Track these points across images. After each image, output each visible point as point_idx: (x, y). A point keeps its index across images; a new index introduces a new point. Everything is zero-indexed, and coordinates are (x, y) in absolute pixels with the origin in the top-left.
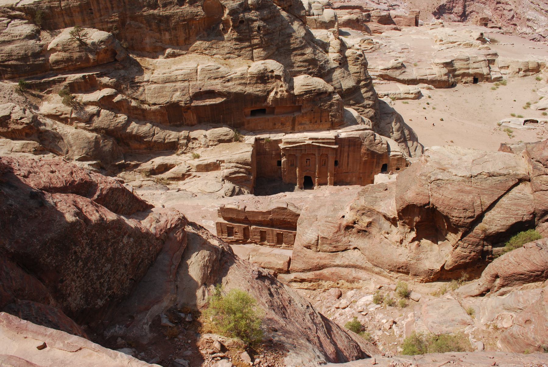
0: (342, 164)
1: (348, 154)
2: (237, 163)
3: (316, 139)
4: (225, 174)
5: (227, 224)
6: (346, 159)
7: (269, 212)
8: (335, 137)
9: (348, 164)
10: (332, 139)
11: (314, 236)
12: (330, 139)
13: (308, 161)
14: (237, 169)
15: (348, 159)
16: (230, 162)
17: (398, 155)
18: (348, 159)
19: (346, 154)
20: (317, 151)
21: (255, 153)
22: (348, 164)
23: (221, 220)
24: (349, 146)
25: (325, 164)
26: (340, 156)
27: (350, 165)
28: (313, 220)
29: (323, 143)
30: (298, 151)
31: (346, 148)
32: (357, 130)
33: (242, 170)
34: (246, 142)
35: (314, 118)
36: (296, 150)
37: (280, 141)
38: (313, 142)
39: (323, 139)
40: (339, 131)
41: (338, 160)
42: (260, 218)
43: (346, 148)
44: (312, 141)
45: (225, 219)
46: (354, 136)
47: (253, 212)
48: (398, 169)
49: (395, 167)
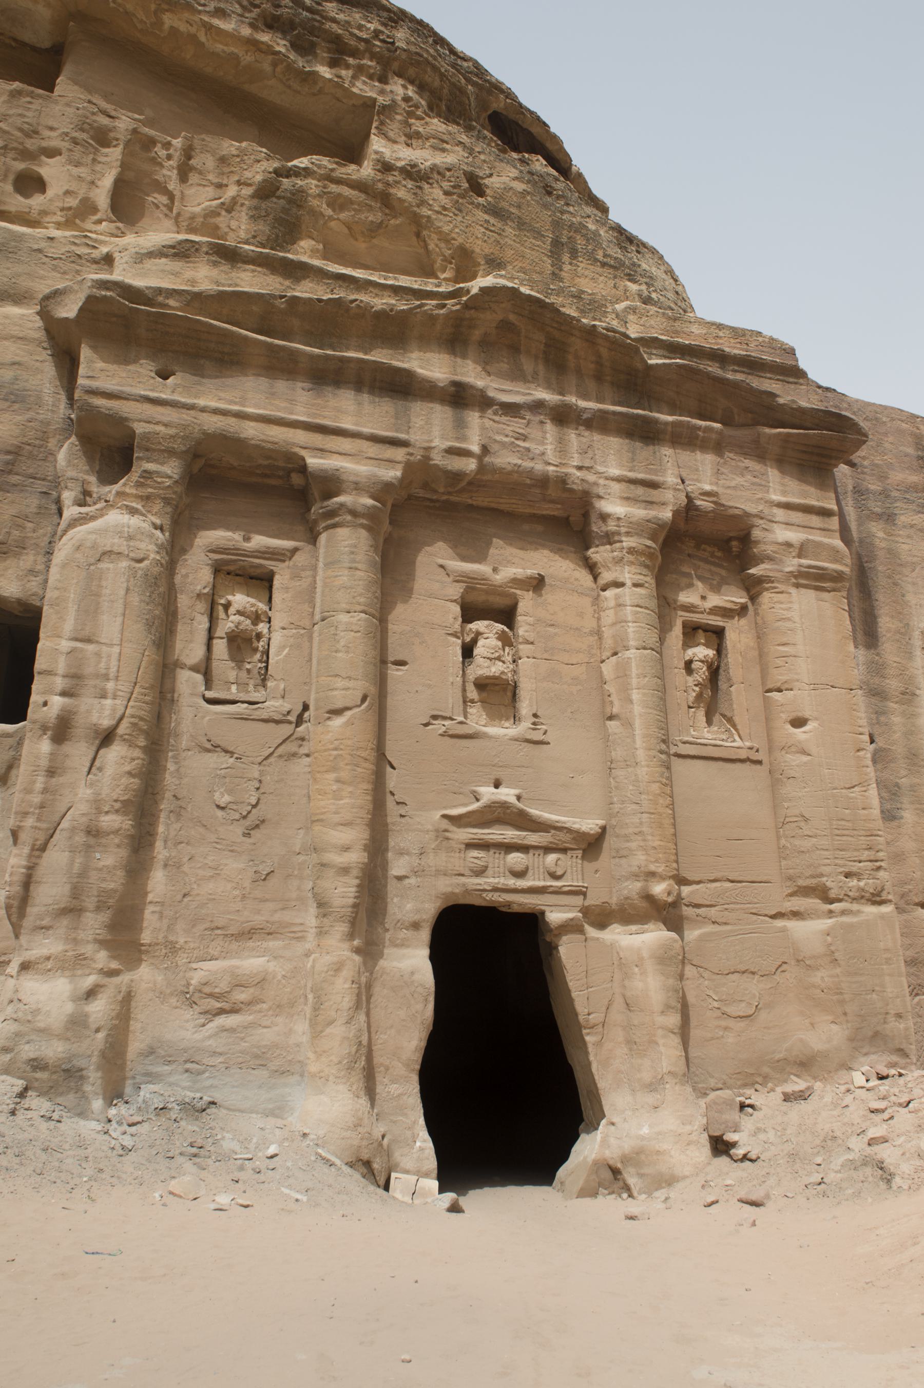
30: (349, 409)
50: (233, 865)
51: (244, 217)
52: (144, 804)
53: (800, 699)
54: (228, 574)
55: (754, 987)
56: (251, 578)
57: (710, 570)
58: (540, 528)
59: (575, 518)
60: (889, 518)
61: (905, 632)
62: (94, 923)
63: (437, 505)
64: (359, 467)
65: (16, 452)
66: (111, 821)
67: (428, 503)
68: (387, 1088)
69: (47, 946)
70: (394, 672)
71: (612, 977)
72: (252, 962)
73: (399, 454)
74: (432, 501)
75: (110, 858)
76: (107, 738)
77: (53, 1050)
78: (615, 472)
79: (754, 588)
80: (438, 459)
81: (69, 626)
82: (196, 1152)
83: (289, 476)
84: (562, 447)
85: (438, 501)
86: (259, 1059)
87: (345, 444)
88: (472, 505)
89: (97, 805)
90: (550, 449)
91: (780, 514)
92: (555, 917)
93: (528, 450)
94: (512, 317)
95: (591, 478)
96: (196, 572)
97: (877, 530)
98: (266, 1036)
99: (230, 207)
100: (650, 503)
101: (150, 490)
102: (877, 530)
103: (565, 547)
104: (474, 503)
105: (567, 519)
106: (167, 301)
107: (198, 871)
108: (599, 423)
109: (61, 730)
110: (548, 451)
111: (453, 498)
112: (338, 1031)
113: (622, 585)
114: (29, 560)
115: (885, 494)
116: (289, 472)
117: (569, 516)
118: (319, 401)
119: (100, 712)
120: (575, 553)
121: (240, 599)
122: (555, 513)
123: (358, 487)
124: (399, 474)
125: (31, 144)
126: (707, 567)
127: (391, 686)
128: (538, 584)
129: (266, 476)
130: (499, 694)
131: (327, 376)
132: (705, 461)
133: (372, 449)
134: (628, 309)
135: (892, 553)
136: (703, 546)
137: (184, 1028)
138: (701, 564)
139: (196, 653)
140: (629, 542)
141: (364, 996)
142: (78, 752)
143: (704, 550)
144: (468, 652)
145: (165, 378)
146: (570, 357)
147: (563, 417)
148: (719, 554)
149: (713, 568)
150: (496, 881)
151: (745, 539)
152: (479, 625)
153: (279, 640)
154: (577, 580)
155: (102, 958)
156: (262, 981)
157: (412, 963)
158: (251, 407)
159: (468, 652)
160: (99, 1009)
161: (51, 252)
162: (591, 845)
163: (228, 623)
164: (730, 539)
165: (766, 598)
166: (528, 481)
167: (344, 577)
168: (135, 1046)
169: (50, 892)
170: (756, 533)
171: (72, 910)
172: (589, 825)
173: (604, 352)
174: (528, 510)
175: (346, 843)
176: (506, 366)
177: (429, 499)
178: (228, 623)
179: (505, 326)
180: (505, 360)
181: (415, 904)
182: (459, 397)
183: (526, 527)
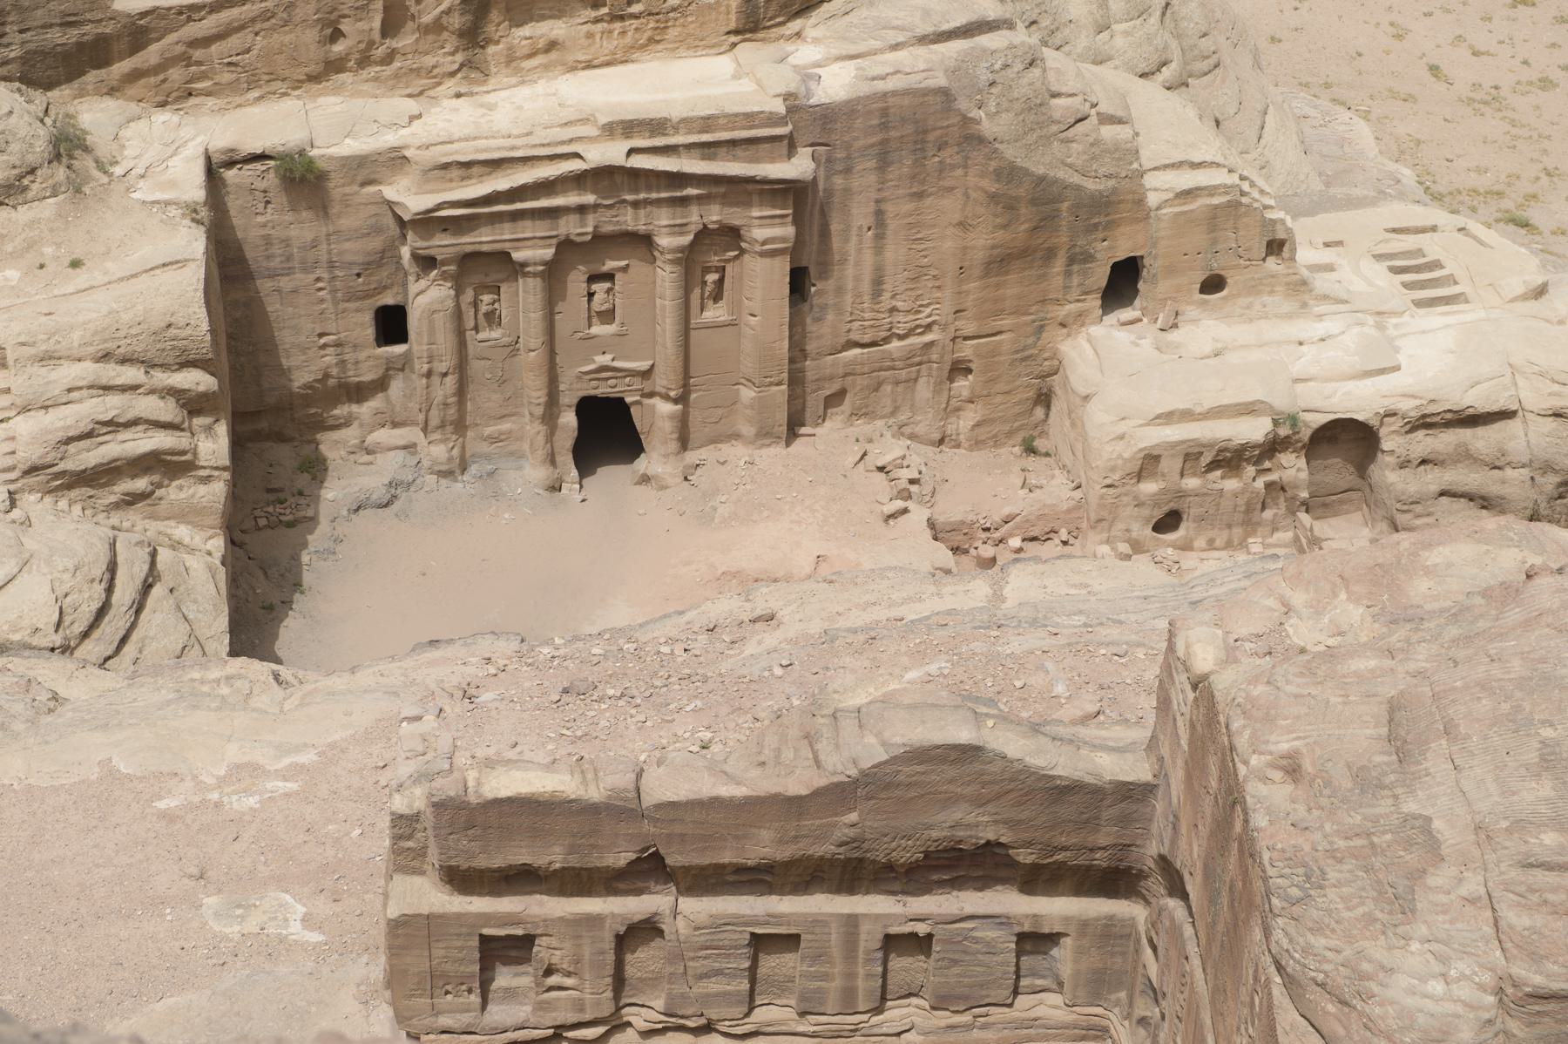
1: (879, 213)
2: (105, 357)
3: (656, 126)
4: (29, 453)
5: (487, 918)
7: (838, 795)
8: (788, 97)
10: (772, 119)
11: (1464, 991)
12: (750, 119)
14: (111, 406)
16: (47, 358)
17: (1211, 191)
21: (216, 273)
23: (426, 895)
24: (883, 164)
28: (1412, 858)
29: (708, 149)
30: (528, 229)
32: (924, 40)
33: (149, 406)
34: (143, 192)
37: (396, 160)
38: (631, 152)
39: (707, 123)
40: (805, 54)
42: (763, 846)
43: (864, 179)
44: (628, 144)
45: (461, 879)
46: (913, 81)
47: (715, 803)
48: (1213, 284)
49: (1201, 276)
50: (495, 397)
51: (456, 14)
52: (461, 392)
53: (755, 306)
55: (720, 411)
60: (848, 171)
61: (848, 228)
62: (449, 429)
64: (535, 253)
65: (383, 251)
66: (451, 400)
68: (559, 459)
69: (436, 436)
70: (557, 317)
71: (656, 415)
72: (506, 426)
73: (554, 241)
75: (452, 411)
76: (445, 375)
77: (444, 468)
78: (665, 222)
79: (743, 251)
80: (572, 237)
82: (495, 495)
84: (636, 219)
86: (512, 454)
89: (446, 397)
90: (629, 218)
91: (756, 222)
92: (628, 400)
96: (469, 295)
97: (838, 181)
98: (513, 448)
99: (448, 12)
100: (681, 234)
102: (838, 181)
107: (484, 399)
108: (658, 202)
109: (429, 374)
110: (630, 220)
112: (540, 452)
114: (395, 289)
115: (849, 157)
119: (443, 367)
121: (487, 298)
123: (535, 264)
124: (552, 251)
125: (333, 17)
127: (557, 325)
128: (625, 269)
130: (608, 316)
131: (516, 216)
132: (715, 208)
133: (541, 242)
135: (847, 191)
137: (484, 448)
139: (471, 324)
140: (669, 257)
141: (550, 437)
142: (436, 379)
147: (636, 205)
150: (603, 390)
152: (595, 287)
153: (504, 310)
155: (454, 437)
156: (510, 432)
157: (569, 419)
158: (483, 239)
159: (591, 295)
160: (456, 452)
161: (381, 159)
162: (646, 374)
163: (484, 308)
165: (746, 257)
167: (531, 299)
168: (468, 454)
169: (434, 421)
171: (442, 426)
172: (643, 365)
175: (540, 396)
178: (484, 308)
181: (569, 398)
182: (582, 209)
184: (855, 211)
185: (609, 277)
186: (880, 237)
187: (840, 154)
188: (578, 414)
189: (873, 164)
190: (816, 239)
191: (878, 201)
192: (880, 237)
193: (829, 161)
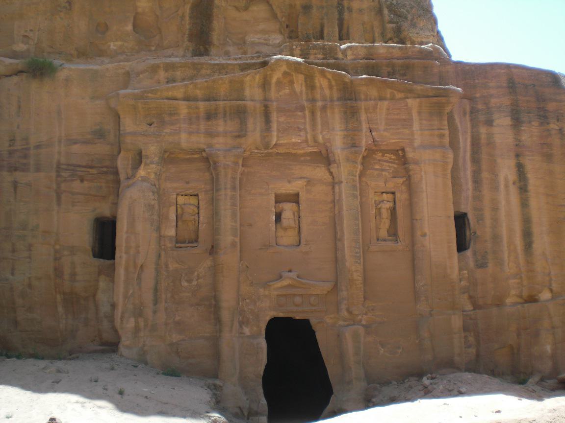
0: (496, 238)
1: (520, 167)
6: (515, 199)
9: (527, 235)
13: (288, 209)
15: (524, 204)
18: (524, 204)
19: (506, 171)
20: (336, 119)
22: (527, 235)
24: (517, 122)
25: (393, 233)
26: (477, 181)
27: (542, 242)
30: (221, 126)
31: (501, 131)
35: (307, 8)
36: (210, 116)
41: (467, 207)
54: (182, 195)
56: (191, 196)
57: (389, 166)
58: (308, 158)
59: (324, 152)
60: (489, 123)
63: (263, 155)
67: (259, 155)
73: (242, 140)
74: (261, 153)
81: (125, 229)
83: (202, 154)
85: (263, 153)
87: (221, 140)
88: (278, 153)
93: (298, 128)
94: (288, 71)
95: (327, 137)
101: (149, 171)
103: (320, 165)
104: (279, 152)
105: (321, 151)
106: (148, 95)
111: (270, 151)
113: (342, 182)
116: (201, 152)
117: (321, 151)
118: (210, 123)
120: (324, 167)
122: (315, 150)
126: (388, 164)
129: (193, 154)
134: (349, 47)
136: (386, 155)
138: (385, 163)
143: (386, 157)
144: (278, 217)
145: (150, 125)
146: (316, 81)
148: (393, 157)
149: (390, 165)
151: (403, 150)
154: (325, 179)
159: (278, 217)
164: (398, 151)
166: (299, 141)
170: (407, 149)
173: (330, 77)
174: (302, 151)
176: (288, 91)
177: (259, 153)
179: (285, 74)
180: (287, 88)
183: (302, 159)
184: (499, 160)
185: (295, 198)
186: (523, 189)
187: (480, 106)
188: (268, 337)
189: (507, 121)
190: (470, 185)
191: (517, 156)
192: (523, 189)
193: (473, 111)
